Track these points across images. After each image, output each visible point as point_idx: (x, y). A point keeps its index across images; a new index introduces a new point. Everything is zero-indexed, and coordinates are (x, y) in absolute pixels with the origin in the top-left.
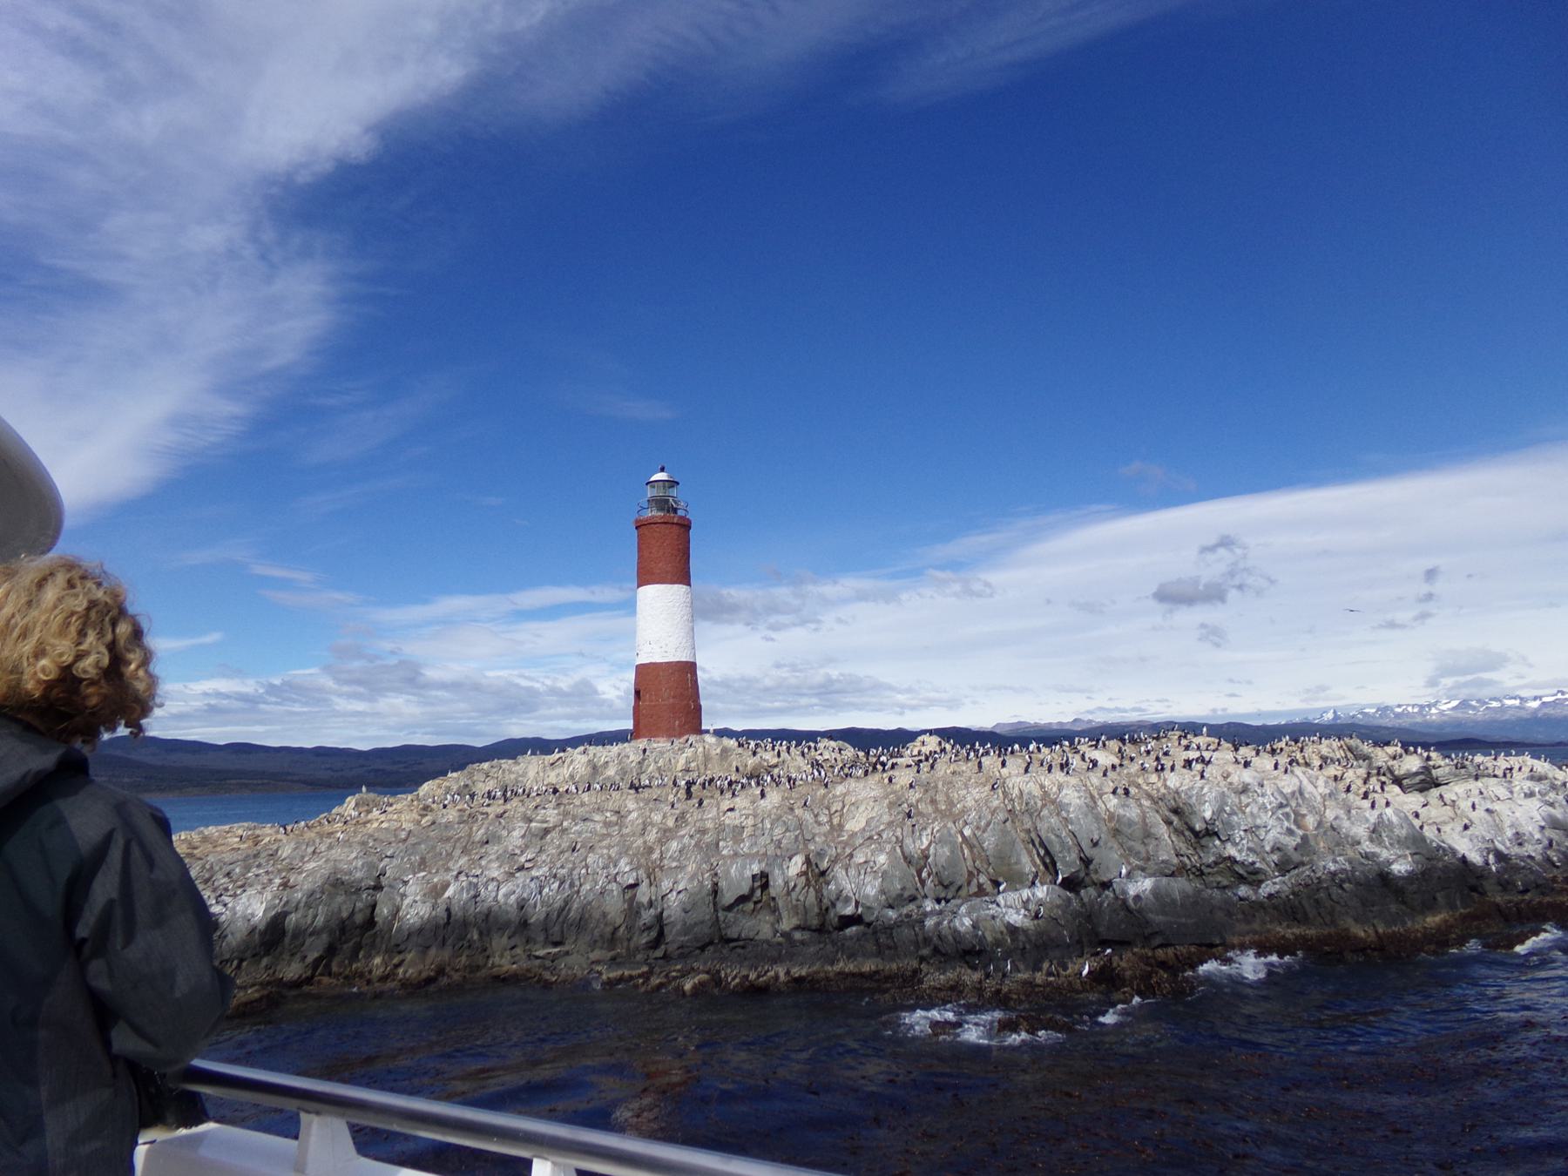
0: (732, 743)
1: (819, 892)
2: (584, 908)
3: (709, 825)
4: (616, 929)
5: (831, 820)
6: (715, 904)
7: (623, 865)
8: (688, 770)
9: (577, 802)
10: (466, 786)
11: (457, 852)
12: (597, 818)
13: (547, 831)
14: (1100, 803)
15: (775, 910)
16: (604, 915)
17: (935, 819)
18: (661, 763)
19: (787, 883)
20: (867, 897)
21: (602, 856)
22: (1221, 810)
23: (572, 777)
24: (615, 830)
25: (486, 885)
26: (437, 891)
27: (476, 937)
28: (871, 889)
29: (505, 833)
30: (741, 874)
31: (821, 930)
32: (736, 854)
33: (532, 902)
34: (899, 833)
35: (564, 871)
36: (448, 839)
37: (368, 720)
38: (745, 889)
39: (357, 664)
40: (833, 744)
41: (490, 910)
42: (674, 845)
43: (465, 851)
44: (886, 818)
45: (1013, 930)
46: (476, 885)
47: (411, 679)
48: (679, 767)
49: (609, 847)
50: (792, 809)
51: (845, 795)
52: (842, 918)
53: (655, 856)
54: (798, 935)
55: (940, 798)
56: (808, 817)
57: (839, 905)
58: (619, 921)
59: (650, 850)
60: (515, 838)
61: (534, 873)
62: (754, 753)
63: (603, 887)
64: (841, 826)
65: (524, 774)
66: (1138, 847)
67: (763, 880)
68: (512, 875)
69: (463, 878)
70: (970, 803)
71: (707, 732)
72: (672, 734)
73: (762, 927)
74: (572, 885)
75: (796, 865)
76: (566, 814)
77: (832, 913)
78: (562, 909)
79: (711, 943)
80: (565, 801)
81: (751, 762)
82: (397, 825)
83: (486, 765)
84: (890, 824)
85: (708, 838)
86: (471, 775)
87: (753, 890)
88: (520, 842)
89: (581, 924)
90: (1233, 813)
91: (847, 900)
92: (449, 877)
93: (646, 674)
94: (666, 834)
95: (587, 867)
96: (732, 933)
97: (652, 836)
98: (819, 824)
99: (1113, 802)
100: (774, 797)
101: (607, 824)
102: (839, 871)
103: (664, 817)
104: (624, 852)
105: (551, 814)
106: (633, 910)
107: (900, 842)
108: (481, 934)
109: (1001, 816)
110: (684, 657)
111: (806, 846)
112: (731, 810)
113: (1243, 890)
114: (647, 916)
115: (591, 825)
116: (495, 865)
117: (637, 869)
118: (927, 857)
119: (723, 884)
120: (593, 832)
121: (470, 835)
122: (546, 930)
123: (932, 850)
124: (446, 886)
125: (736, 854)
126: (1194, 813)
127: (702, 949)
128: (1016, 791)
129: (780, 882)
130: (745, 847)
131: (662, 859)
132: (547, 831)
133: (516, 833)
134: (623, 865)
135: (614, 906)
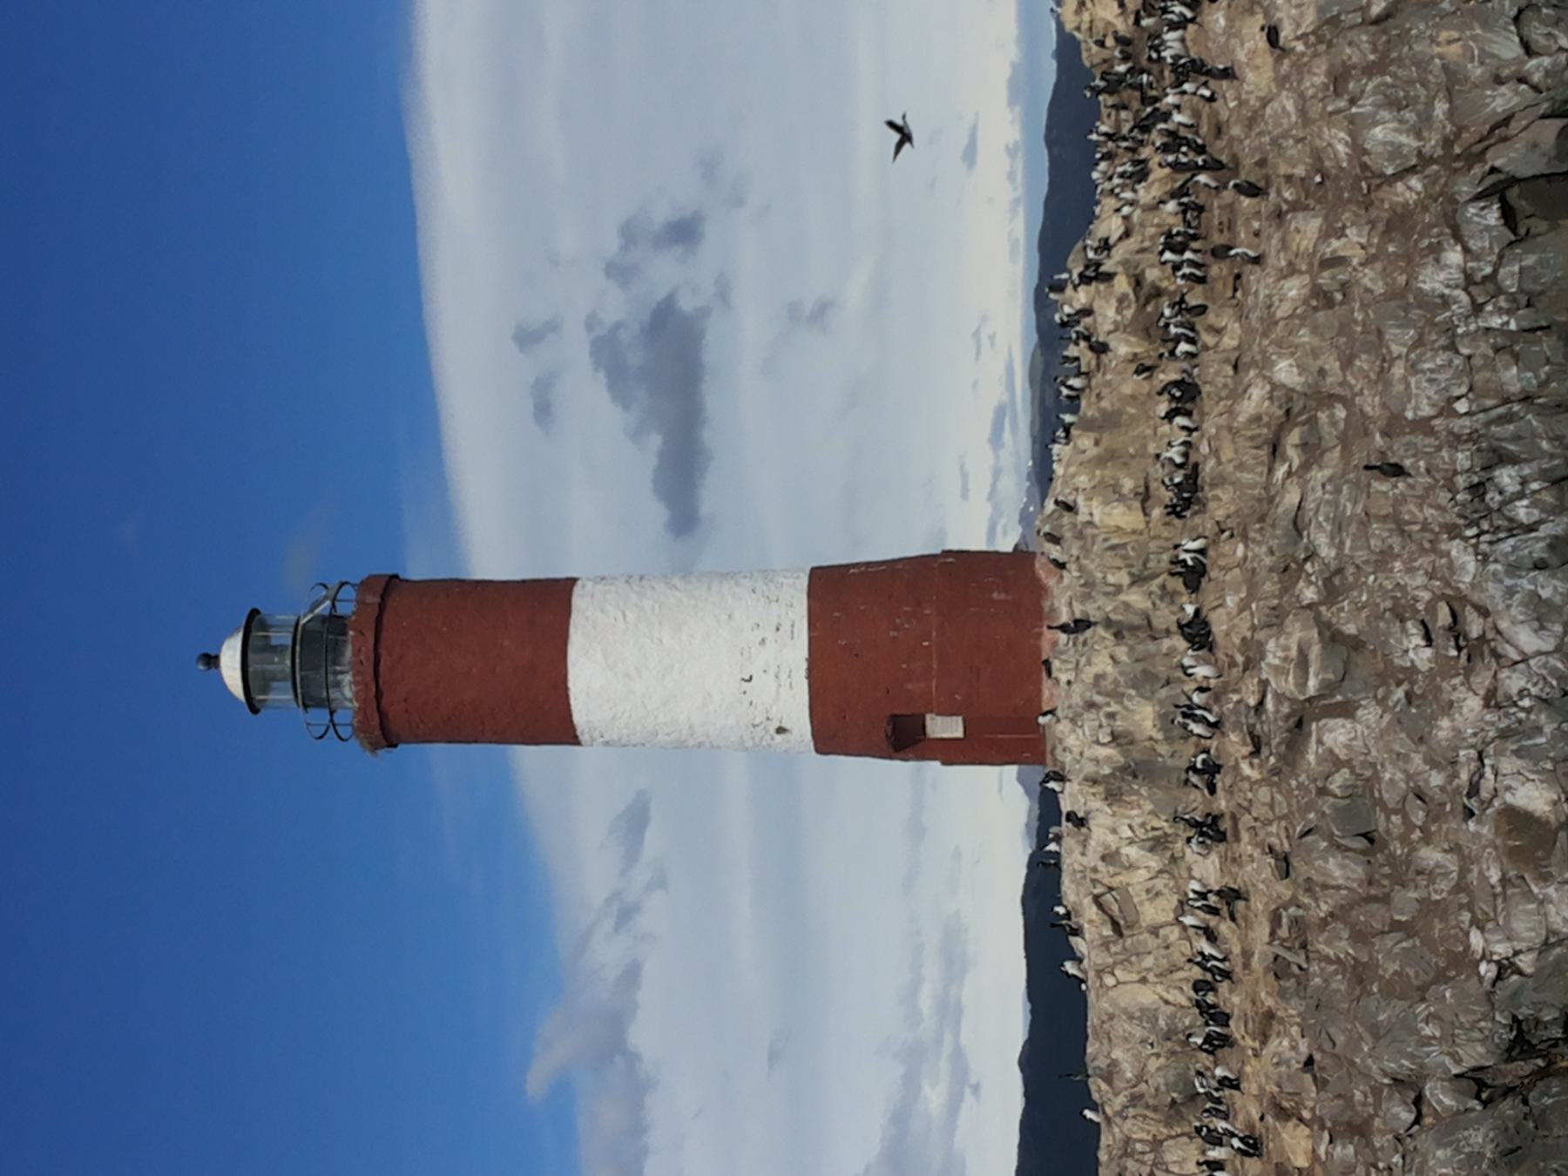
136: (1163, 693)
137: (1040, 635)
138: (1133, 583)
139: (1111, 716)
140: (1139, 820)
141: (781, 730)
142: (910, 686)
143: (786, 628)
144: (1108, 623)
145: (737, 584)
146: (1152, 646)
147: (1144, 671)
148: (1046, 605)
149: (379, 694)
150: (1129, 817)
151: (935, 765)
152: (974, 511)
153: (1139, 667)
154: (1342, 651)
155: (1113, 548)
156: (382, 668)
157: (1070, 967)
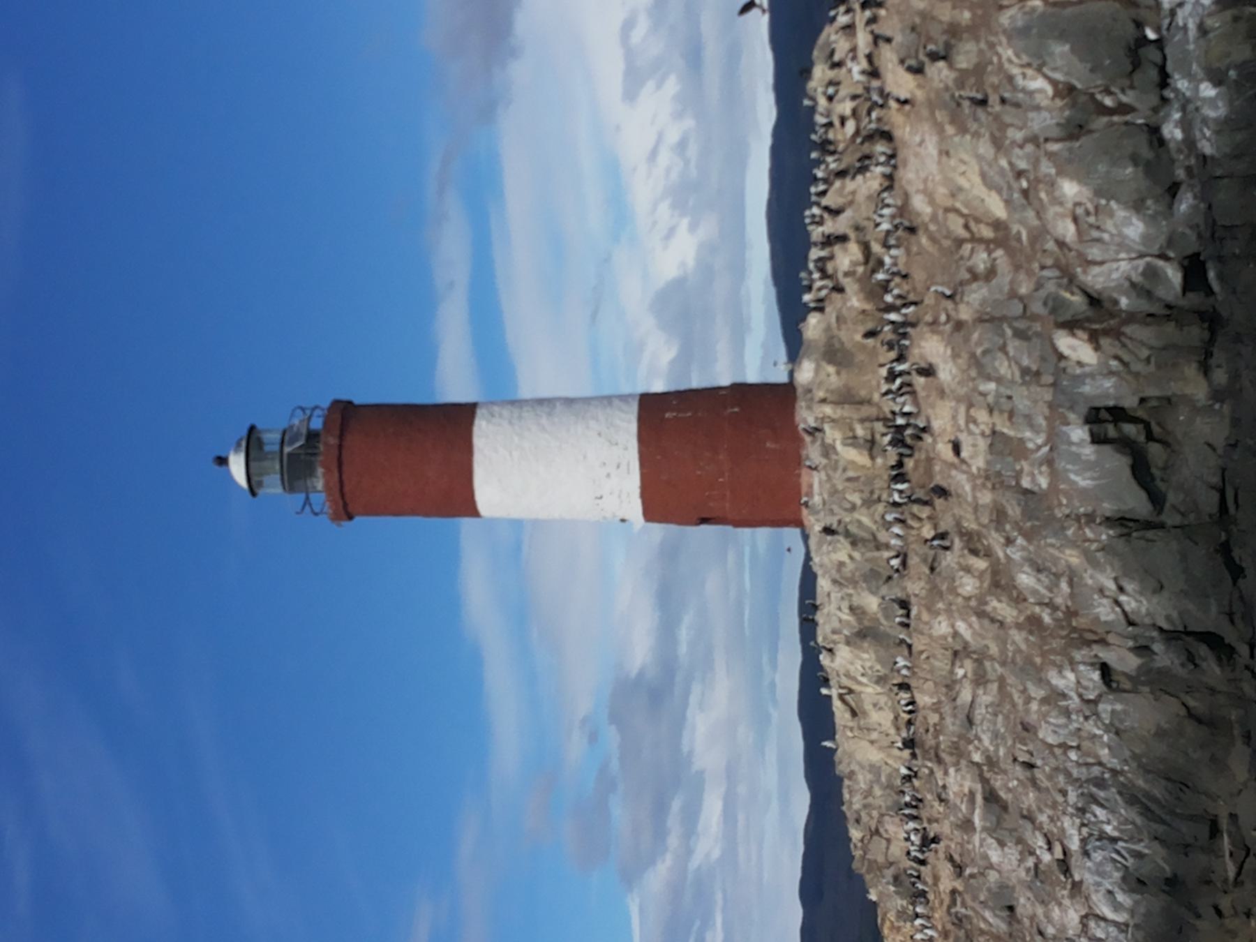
0: (813, 326)
1: (1131, 318)
2: (1145, 770)
3: (986, 498)
4: (1191, 714)
6: (1148, 525)
7: (1065, 680)
8: (871, 445)
9: (934, 718)
10: (896, 880)
12: (966, 695)
13: (991, 797)
15: (1169, 401)
16: (1160, 734)
17: (992, 46)
18: (856, 498)
19: (1111, 373)
20: (1146, 238)
23: (880, 680)
24: (994, 669)
28: (1135, 229)
30: (1087, 466)
31: (1212, 320)
32: (1049, 462)
34: (1019, 136)
35: (1072, 796)
37: (742, 789)
38: (1119, 463)
39: (619, 812)
40: (820, 73)
42: (1025, 579)
44: (985, 148)
47: (653, 697)
50: (959, 325)
52: (1187, 287)
53: (1047, 619)
54: (1220, 377)
56: (976, 295)
57: (1161, 292)
58: (1173, 706)
59: (1033, 623)
60: (1003, 859)
61: (1074, 845)
62: (839, 289)
63: (1107, 729)
64: (997, 225)
65: (874, 769)
67: (1104, 421)
68: (1076, 888)
71: (791, 373)
72: (793, 461)
73: (1201, 431)
74: (1100, 783)
77: (1183, 303)
78: (1146, 812)
79: (1225, 549)
80: (930, 741)
81: (855, 301)
83: (855, 834)
84: (998, 143)
85: (1014, 511)
86: (875, 867)
87: (1124, 444)
88: (1013, 852)
89: (1180, 782)
91: (1151, 273)
94: (1000, 581)
95: (1065, 747)
96: (1209, 502)
97: (1001, 608)
98: (991, 273)
100: (930, 347)
101: (980, 680)
102: (1095, 279)
103: (968, 570)
104: (1032, 670)
105: (958, 782)
106: (1153, 681)
107: (1033, 139)
110: (627, 426)
111: (1035, 318)
112: (957, 448)
114: (1164, 657)
116: (1056, 913)
117: (1073, 664)
118: (1071, 89)
119: (1108, 508)
120: (996, 708)
122: (1186, 848)
123: (1058, 76)
125: (1049, 462)
127: (1237, 572)
129: (1108, 384)
130: (1035, 440)
132: (991, 797)
133: (995, 856)
134: (1065, 680)
135: (1143, 713)
136: (884, 590)
137: (799, 476)
138: (863, 505)
139: (850, 595)
140: (868, 664)
141: (623, 521)
142: (711, 504)
143: (624, 467)
144: (847, 534)
145: (588, 427)
146: (876, 554)
147: (871, 570)
148: (804, 453)
149: (345, 505)
150: (861, 659)
151: (729, 528)
152: (754, 357)
153: (868, 566)
154: (996, 808)
155: (849, 480)
156: (346, 489)
157: (824, 691)
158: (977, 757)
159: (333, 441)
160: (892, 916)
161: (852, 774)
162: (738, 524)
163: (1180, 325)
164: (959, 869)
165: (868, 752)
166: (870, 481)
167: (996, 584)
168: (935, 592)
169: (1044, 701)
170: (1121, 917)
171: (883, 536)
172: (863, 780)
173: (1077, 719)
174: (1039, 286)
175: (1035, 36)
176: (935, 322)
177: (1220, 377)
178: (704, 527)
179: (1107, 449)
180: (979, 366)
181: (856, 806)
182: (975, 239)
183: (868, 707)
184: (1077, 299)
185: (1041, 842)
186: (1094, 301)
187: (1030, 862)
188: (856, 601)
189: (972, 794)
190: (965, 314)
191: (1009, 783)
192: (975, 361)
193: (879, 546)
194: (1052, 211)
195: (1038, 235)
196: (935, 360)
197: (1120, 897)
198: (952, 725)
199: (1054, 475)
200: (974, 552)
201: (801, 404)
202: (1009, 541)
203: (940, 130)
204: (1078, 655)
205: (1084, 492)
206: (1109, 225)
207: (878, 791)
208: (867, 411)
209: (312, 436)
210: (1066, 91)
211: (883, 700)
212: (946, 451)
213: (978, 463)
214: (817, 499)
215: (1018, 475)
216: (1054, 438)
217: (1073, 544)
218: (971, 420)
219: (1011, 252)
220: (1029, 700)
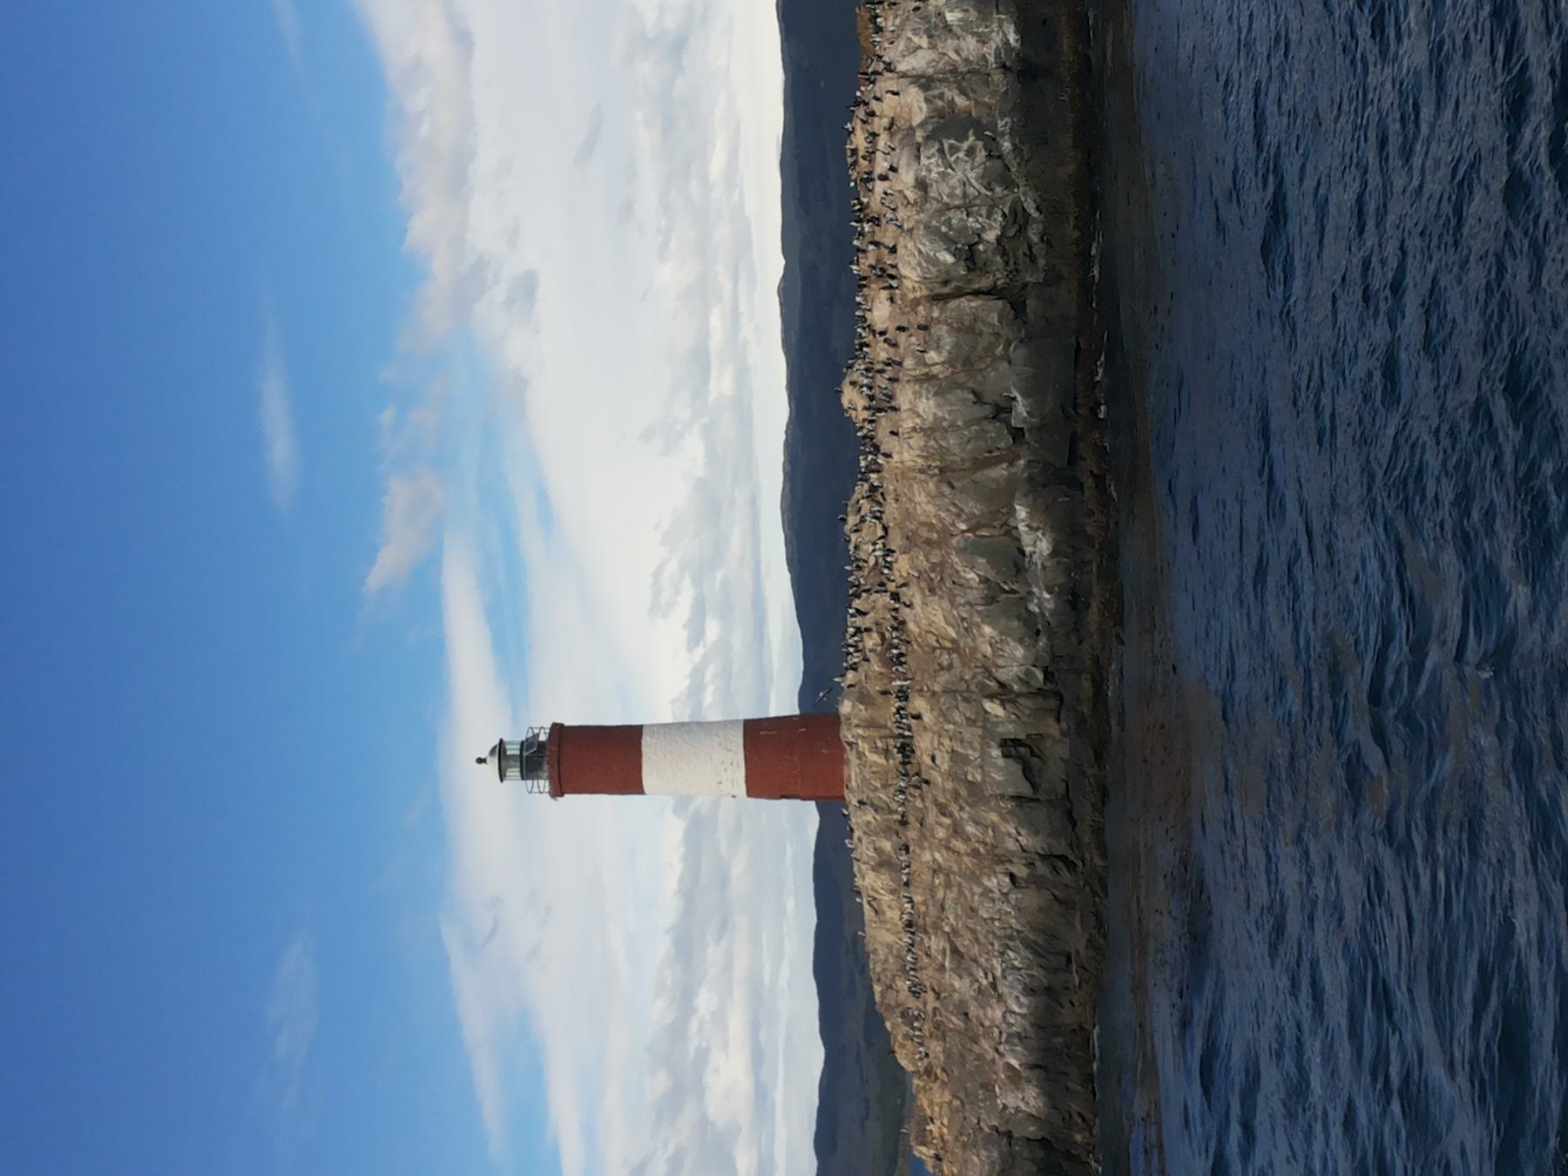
1: (1020, 695)
2: (1033, 929)
5: (948, 650)
6: (1031, 800)
7: (991, 883)
8: (886, 752)
9: (923, 909)
11: (976, 1049)
12: (940, 895)
13: (955, 951)
14: (936, 370)
16: (1041, 909)
20: (1025, 657)
21: (982, 903)
22: (945, 238)
23: (892, 892)
24: (956, 879)
25: (1010, 1025)
26: (1014, 1077)
27: (1060, 1040)
28: (1020, 652)
29: (956, 996)
30: (1000, 769)
33: (1027, 980)
35: (997, 946)
36: (962, 1056)
38: (1016, 768)
41: (1032, 1025)
42: (970, 829)
43: (975, 1041)
44: (946, 604)
45: (1055, 553)
46: (1009, 1035)
48: (882, 761)
49: (973, 894)
50: (934, 694)
51: (917, 624)
52: (1046, 677)
54: (1064, 725)
55: (924, 533)
57: (1033, 683)
58: (1048, 896)
59: (975, 853)
60: (961, 985)
61: (998, 973)
62: (867, 660)
63: (1013, 907)
64: (953, 641)
65: (889, 946)
66: (983, 342)
67: (1010, 746)
68: (1000, 997)
69: (1001, 1048)
70: (930, 508)
72: (839, 760)
75: (994, 708)
76: (937, 927)
78: (1035, 952)
79: (1069, 813)
80: (921, 922)
81: (876, 667)
82: (945, 1109)
83: (877, 988)
84: (952, 603)
85: (963, 792)
86: (890, 1008)
87: (1019, 759)
88: (967, 981)
89: (1051, 935)
90: (948, 223)
91: (1028, 673)
92: (1000, 1063)
93: (762, 783)
94: (957, 830)
95: (992, 919)
96: (1061, 788)
97: (959, 845)
98: (951, 666)
99: (932, 356)
100: (919, 704)
101: (948, 885)
102: (1002, 675)
103: (941, 824)
104: (974, 878)
105: (936, 943)
106: (1035, 881)
107: (969, 603)
108: (1057, 1035)
109: (946, 490)
113: (1033, 234)
114: (1042, 869)
115: (948, 904)
118: (987, 580)
119: (1011, 791)
120: (956, 901)
121: (959, 1032)
122: (1056, 970)
124: (1009, 1066)
125: (981, 767)
126: (947, 272)
128: (920, 461)
131: (985, 844)
132: (955, 951)
133: (957, 984)
134: (991, 883)
135: (1031, 899)
144: (872, 805)
151: (799, 802)
158: (947, 929)
159: (555, 749)
160: (900, 1038)
161: (875, 952)
162: (803, 799)
163: (1045, 698)
164: (938, 996)
165: (883, 936)
166: (886, 773)
167: (956, 832)
168: (923, 837)
169: (982, 895)
170: (1024, 1011)
171: (894, 806)
172: (882, 954)
173: (997, 902)
174: (974, 677)
175: (971, 550)
176: (921, 690)
177: (1064, 725)
178: (784, 801)
179: (1010, 761)
180: (944, 716)
181: (878, 970)
182: (942, 648)
183: (886, 908)
184: (993, 684)
185: (981, 974)
186: (1001, 685)
187: (976, 986)
188: (878, 844)
189: (944, 950)
190: (937, 688)
191: (963, 943)
192: (942, 714)
193: (891, 812)
194: (979, 640)
195: (974, 650)
196: (923, 711)
197: (1022, 999)
198: (933, 911)
199: (984, 774)
200: (944, 815)
201: (844, 727)
202: (962, 809)
203: (923, 592)
204: (998, 868)
205: (999, 782)
206: (1007, 648)
207: (891, 960)
208: (883, 732)
209: (541, 745)
210: (985, 580)
211: (894, 904)
212: (928, 761)
213: (945, 767)
214: (853, 784)
215: (966, 774)
216: (984, 755)
217: (994, 810)
218: (941, 744)
219: (960, 655)
220: (973, 894)
